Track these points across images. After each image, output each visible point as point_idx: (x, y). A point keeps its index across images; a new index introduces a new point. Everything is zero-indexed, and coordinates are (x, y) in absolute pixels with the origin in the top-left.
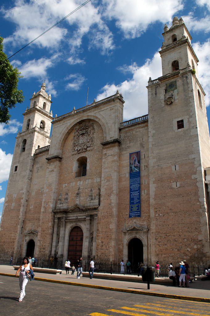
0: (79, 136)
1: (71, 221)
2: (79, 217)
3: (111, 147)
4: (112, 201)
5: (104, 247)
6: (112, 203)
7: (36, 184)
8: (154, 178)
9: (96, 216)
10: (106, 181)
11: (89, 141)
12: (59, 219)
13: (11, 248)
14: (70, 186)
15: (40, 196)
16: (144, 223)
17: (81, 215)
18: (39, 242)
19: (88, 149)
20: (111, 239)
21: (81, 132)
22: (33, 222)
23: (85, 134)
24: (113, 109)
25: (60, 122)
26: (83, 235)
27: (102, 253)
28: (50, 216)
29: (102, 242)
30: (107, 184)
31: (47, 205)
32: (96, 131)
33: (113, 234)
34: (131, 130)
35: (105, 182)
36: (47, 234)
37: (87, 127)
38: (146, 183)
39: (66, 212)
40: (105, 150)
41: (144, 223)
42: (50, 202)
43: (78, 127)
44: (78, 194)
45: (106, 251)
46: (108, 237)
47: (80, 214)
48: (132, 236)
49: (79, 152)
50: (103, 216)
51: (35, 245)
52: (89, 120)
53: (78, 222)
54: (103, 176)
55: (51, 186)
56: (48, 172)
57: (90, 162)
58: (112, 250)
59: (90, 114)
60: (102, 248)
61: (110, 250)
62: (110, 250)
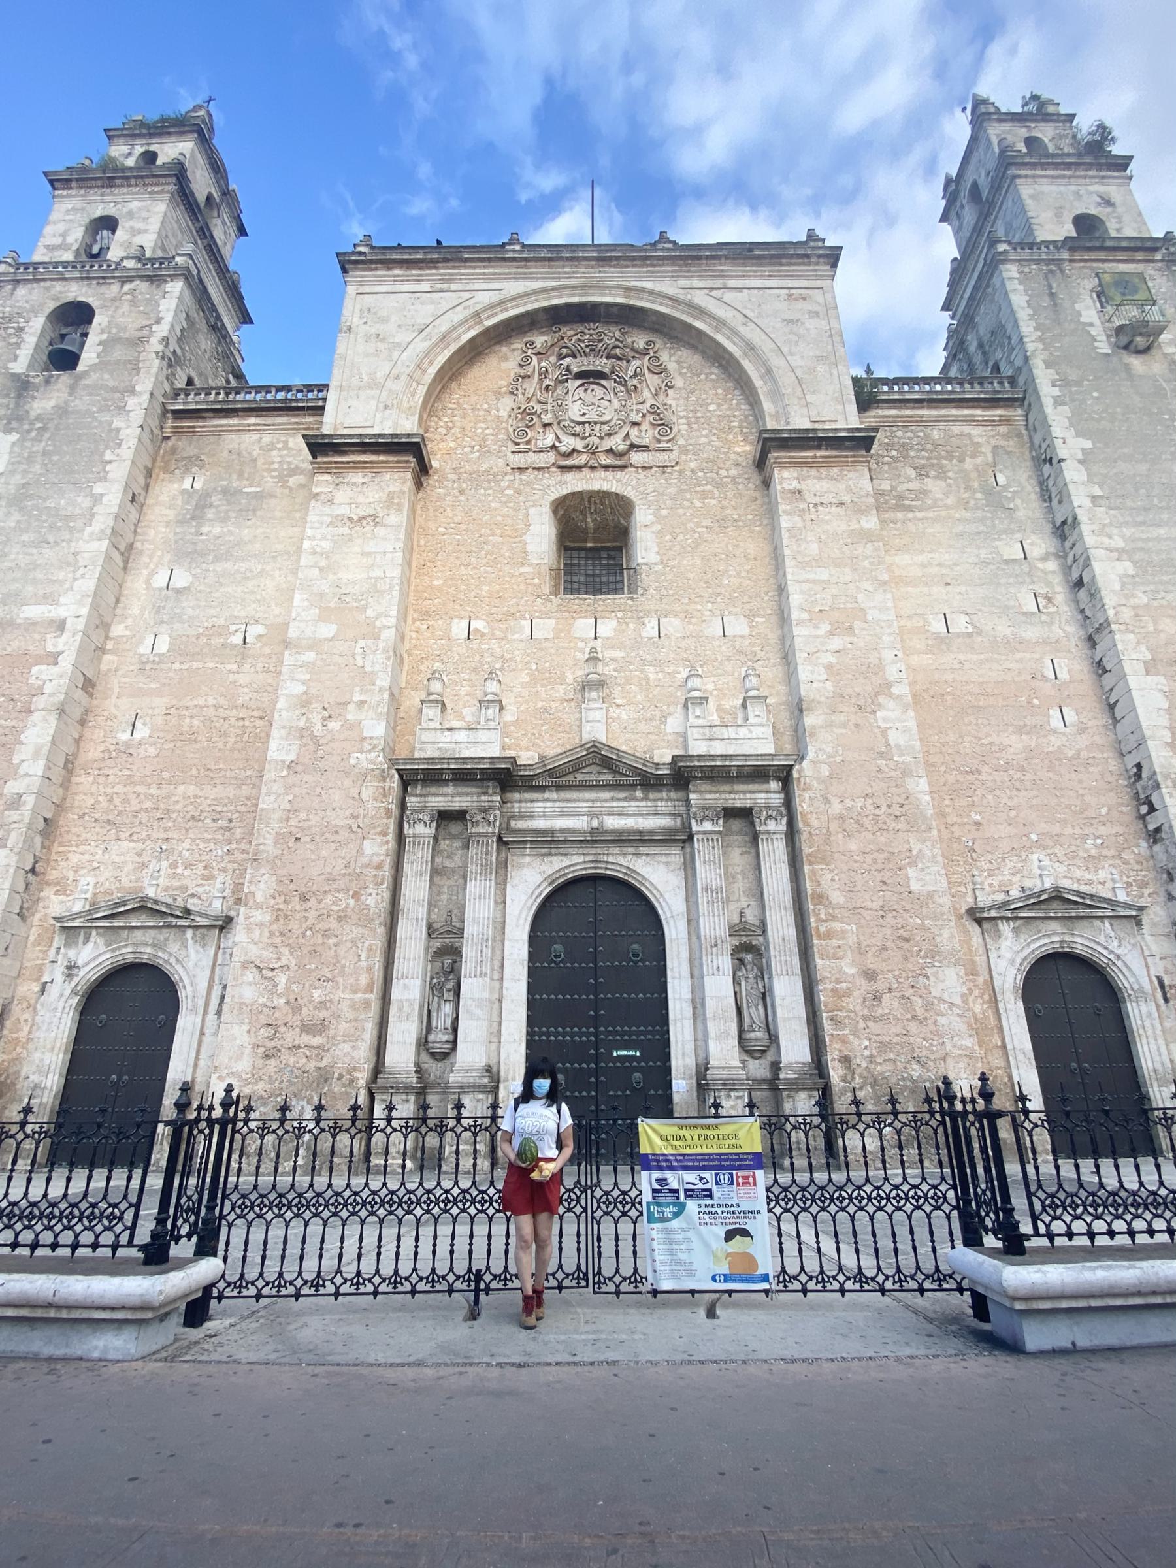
0: (559, 382)
1: (549, 842)
2: (611, 823)
3: (827, 463)
4: (894, 737)
6: (894, 750)
7: (179, 591)
8: (1143, 648)
9: (769, 817)
10: (825, 628)
11: (635, 417)
14: (516, 636)
15: (234, 667)
16: (1103, 875)
17: (632, 806)
18: (250, 976)
19: (636, 457)
22: (163, 835)
23: (603, 382)
24: (804, 299)
26: (663, 934)
27: (884, 1046)
29: (870, 976)
30: (836, 643)
31: (334, 725)
32: (679, 382)
33: (941, 927)
34: (921, 420)
35: (821, 632)
36: (340, 919)
37: (618, 351)
38: (1063, 675)
40: (786, 474)
41: (1103, 875)
42: (363, 702)
43: (540, 340)
44: (585, 686)
45: (913, 1027)
46: (907, 940)
47: (615, 804)
48: (1046, 941)
49: (566, 463)
50: (841, 817)
51: (183, 1006)
53: (617, 850)
54: (795, 598)
56: (328, 519)
57: (659, 527)
58: (951, 1021)
59: (648, 285)
60: (880, 1011)
61: (942, 1020)
62: (942, 1020)
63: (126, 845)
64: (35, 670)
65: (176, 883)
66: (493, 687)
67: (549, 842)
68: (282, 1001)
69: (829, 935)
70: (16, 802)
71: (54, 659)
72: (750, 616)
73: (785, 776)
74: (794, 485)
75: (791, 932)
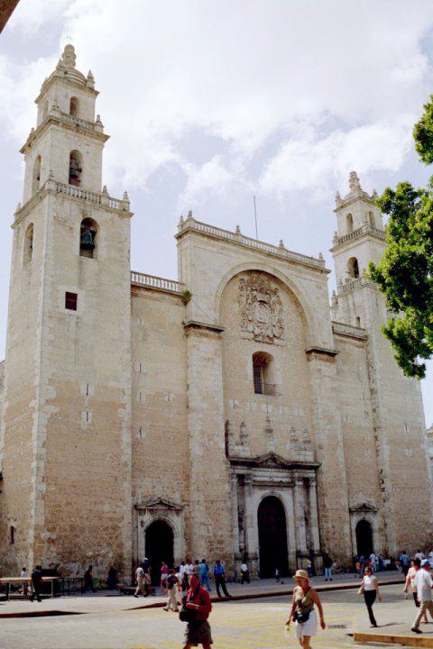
1: (262, 485)
2: (276, 480)
3: (327, 360)
5: (337, 534)
11: (274, 323)
12: (241, 478)
13: (109, 545)
17: (280, 474)
19: (276, 340)
20: (345, 522)
21: (260, 297)
25: (212, 241)
28: (220, 470)
29: (334, 527)
31: (211, 443)
34: (345, 342)
36: (222, 510)
39: (252, 464)
43: (246, 278)
52: (273, 277)
55: (213, 397)
63: (148, 479)
64: (120, 410)
65: (165, 494)
66: (244, 429)
67: (262, 485)
68: (211, 535)
69: (326, 517)
70: (126, 465)
71: (123, 406)
72: (304, 409)
73: (316, 468)
74: (319, 367)
75: (316, 516)
